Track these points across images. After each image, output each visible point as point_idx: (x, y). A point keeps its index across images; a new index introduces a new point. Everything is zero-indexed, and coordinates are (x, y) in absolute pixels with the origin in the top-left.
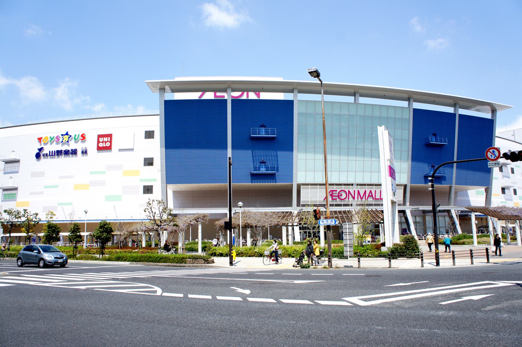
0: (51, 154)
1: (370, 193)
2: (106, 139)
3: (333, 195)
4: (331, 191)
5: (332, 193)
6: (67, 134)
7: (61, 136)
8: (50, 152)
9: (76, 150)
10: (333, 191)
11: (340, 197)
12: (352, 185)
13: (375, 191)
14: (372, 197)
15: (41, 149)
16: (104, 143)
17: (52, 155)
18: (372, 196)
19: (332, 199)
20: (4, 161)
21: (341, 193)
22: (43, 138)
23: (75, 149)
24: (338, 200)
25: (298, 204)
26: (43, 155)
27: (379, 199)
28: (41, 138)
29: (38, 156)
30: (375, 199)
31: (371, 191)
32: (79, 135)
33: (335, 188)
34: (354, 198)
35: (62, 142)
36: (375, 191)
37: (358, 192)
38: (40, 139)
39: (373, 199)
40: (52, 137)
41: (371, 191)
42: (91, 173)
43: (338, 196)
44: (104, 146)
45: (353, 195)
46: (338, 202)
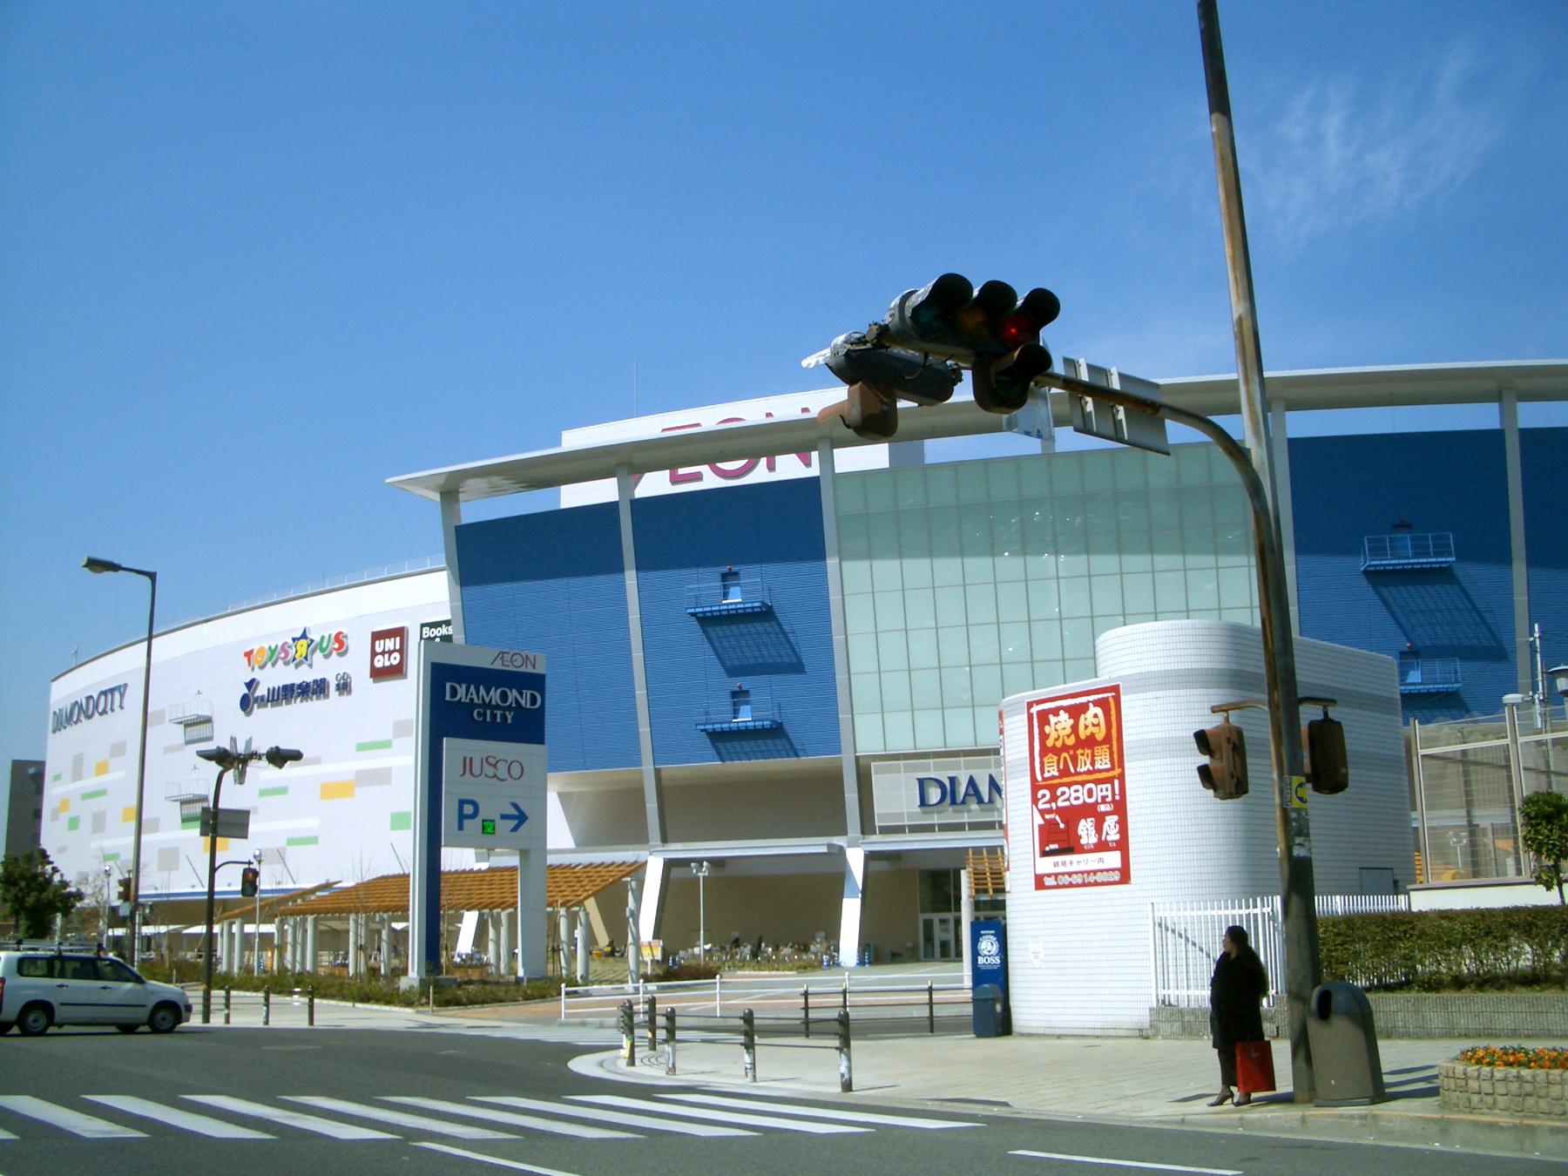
0: (270, 699)
2: (390, 644)
6: (304, 636)
7: (290, 642)
8: (269, 690)
9: (323, 681)
15: (251, 684)
16: (387, 656)
17: (273, 700)
20: (181, 723)
22: (255, 652)
23: (321, 680)
25: (867, 827)
26: (256, 700)
28: (252, 651)
29: (246, 704)
32: (330, 636)
35: (294, 659)
38: (248, 655)
40: (273, 648)
42: (362, 747)
44: (387, 664)
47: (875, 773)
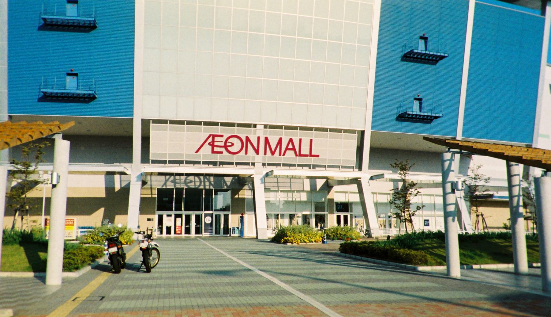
1: (291, 144)
3: (216, 144)
4: (210, 136)
5: (213, 141)
10: (214, 136)
11: (229, 148)
12: (255, 126)
13: (300, 140)
14: (293, 152)
18: (294, 149)
19: (213, 152)
21: (231, 140)
24: (225, 153)
27: (306, 156)
30: (300, 155)
31: (291, 141)
33: (219, 130)
34: (257, 152)
36: (300, 140)
37: (267, 140)
39: (296, 155)
41: (291, 141)
43: (225, 147)
45: (256, 145)
46: (225, 157)
47: (152, 130)
